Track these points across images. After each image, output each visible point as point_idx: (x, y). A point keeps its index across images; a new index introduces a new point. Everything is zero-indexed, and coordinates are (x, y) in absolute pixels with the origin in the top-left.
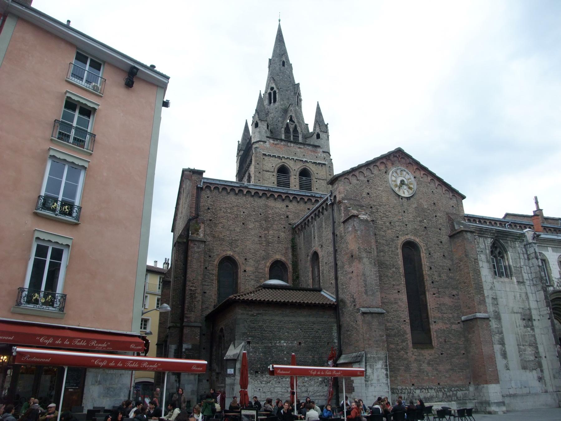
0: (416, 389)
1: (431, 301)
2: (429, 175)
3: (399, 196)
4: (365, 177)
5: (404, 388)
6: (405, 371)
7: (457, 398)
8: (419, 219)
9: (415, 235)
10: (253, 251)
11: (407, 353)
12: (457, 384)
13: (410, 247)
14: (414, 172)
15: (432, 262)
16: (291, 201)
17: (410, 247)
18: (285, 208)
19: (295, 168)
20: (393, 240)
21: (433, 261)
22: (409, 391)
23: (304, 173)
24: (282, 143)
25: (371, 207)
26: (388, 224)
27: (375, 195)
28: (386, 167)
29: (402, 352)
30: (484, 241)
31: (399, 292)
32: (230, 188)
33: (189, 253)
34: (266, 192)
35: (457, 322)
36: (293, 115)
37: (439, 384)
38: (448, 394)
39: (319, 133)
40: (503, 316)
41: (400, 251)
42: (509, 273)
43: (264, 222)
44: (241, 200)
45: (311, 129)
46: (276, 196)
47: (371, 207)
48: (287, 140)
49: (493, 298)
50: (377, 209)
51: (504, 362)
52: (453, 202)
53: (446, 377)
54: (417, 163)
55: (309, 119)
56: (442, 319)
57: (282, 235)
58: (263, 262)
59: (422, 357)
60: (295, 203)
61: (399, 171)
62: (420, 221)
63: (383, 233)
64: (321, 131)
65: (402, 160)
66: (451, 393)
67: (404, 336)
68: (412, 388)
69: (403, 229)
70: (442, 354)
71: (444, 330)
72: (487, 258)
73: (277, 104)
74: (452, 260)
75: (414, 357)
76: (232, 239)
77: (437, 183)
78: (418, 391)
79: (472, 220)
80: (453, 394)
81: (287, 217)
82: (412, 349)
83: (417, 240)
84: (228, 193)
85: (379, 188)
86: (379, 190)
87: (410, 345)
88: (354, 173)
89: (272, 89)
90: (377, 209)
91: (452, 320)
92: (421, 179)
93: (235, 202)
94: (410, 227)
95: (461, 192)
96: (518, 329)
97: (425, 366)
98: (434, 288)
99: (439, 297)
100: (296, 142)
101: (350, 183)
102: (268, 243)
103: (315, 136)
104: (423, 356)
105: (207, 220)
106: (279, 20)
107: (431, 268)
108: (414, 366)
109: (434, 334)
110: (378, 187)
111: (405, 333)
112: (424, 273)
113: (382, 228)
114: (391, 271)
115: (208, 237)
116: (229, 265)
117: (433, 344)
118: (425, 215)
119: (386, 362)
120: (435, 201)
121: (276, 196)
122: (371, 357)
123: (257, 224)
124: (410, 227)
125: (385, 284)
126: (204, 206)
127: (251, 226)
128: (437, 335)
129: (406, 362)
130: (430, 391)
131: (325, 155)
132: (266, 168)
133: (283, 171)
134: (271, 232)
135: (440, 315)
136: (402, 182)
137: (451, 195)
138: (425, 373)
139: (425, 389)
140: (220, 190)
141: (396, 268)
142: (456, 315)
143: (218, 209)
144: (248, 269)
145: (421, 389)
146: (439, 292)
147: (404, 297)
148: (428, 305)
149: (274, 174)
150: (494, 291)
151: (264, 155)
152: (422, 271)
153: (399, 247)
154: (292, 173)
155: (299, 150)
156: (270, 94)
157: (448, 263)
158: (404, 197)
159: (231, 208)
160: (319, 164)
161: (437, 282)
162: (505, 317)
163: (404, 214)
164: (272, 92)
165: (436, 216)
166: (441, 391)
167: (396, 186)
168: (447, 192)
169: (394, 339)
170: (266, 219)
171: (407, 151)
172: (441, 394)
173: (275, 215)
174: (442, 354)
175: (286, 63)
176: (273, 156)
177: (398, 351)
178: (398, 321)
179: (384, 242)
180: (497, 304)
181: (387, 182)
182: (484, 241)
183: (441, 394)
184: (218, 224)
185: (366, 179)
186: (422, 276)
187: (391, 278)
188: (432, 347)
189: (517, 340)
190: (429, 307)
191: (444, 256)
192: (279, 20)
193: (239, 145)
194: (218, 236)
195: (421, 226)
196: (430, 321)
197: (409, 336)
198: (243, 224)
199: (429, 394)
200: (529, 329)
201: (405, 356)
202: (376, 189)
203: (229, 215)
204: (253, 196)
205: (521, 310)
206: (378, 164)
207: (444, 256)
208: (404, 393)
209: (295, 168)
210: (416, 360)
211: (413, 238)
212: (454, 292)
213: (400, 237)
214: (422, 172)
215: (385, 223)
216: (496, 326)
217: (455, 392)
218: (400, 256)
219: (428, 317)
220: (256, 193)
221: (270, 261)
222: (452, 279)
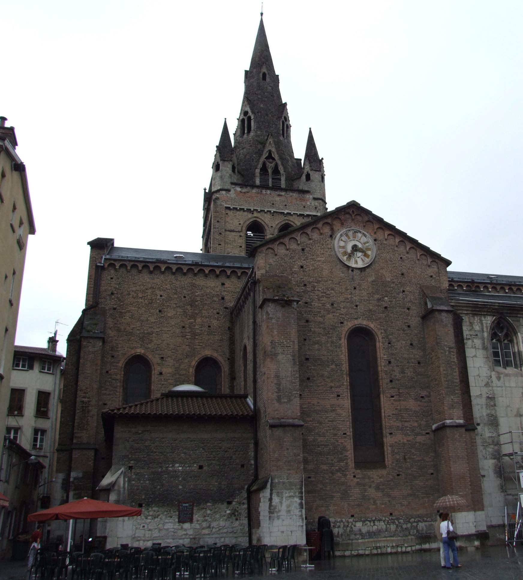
0: (356, 522)
1: (387, 406)
2: (396, 236)
3: (348, 267)
4: (298, 244)
5: (339, 520)
7: (418, 531)
8: (376, 297)
10: (172, 346)
11: (345, 475)
12: (418, 513)
13: (361, 337)
14: (375, 233)
15: (392, 354)
16: (228, 277)
17: (361, 337)
18: (220, 287)
20: (334, 328)
22: (346, 524)
24: (254, 191)
25: (305, 285)
26: (328, 306)
27: (311, 268)
28: (332, 229)
29: (339, 474)
31: (338, 396)
32: (142, 264)
33: (82, 354)
34: (193, 267)
35: (424, 432)
36: (273, 150)
37: (391, 514)
38: (404, 526)
39: (310, 172)
41: (344, 342)
42: (518, 363)
43: (189, 307)
44: (158, 279)
46: (207, 272)
47: (305, 285)
48: (264, 186)
49: (488, 397)
50: (314, 287)
52: (434, 268)
53: (402, 505)
54: (379, 220)
55: (299, 151)
56: (402, 429)
57: (215, 323)
58: (186, 361)
60: (234, 279)
61: (350, 234)
62: (379, 300)
63: (321, 319)
64: (312, 170)
65: (358, 217)
66: (409, 525)
67: (342, 454)
68: (351, 520)
69: (351, 311)
70: (398, 475)
71: (404, 444)
72: (484, 344)
73: (252, 134)
74: (424, 350)
75: (355, 480)
76: (144, 333)
77: (409, 246)
78: (359, 525)
79: (498, 287)
80: (412, 526)
81: (223, 298)
82: (354, 470)
83: (372, 325)
84: (140, 272)
85: (319, 259)
86: (319, 261)
87: (351, 464)
88: (281, 240)
90: (314, 287)
91: (417, 430)
92: (385, 242)
93: (149, 282)
94: (362, 308)
95: (444, 255)
97: (372, 492)
98: (393, 388)
99: (400, 400)
101: (276, 255)
102: (194, 335)
104: (369, 478)
105: (109, 310)
107: (390, 362)
108: (355, 492)
109: (388, 450)
110: (318, 256)
111: (345, 449)
112: (379, 369)
113: (319, 312)
114: (328, 369)
115: (110, 332)
116: (139, 365)
117: (386, 463)
118: (386, 291)
119: (301, 488)
120: (404, 271)
121: (207, 272)
122: (279, 482)
123: (179, 310)
124: (362, 308)
125: (318, 386)
126: (105, 291)
127: (171, 313)
128: (393, 451)
129: (343, 488)
130: (376, 523)
131: (316, 203)
132: (229, 227)
134: (199, 320)
135: (399, 424)
136: (355, 248)
137: (430, 260)
138: (372, 501)
139: (370, 521)
140: (129, 268)
141: (336, 365)
142: (423, 423)
143: (126, 293)
144: (164, 370)
145: (364, 522)
146: (400, 394)
147: (347, 403)
148: (383, 411)
149: (241, 234)
150: (490, 388)
152: (377, 366)
153: (343, 336)
155: (278, 199)
157: (417, 354)
158: (356, 269)
159: (143, 292)
161: (398, 380)
163: (354, 292)
165: (404, 291)
167: (345, 253)
168: (424, 257)
169: (327, 458)
170: (192, 304)
171: (364, 204)
172: (393, 527)
173: (205, 297)
174: (398, 475)
175: (267, 76)
176: (241, 209)
177: (332, 474)
178: (335, 435)
179: (321, 331)
180: (495, 405)
181: (333, 249)
182: (481, 321)
183: (393, 527)
184: (125, 313)
185: (300, 248)
186: (376, 373)
187: (328, 378)
188: (384, 467)
190: (383, 414)
191: (411, 344)
194: (125, 329)
195: (378, 306)
196: (384, 432)
197: (350, 453)
198: (160, 311)
199: (375, 528)
201: (343, 479)
202: (313, 259)
203: (140, 300)
204: (174, 274)
206: (320, 225)
207: (411, 344)
208: (339, 527)
210: (358, 484)
211: (365, 323)
212: (424, 393)
213: (345, 323)
214: (387, 232)
215: (323, 305)
216: (490, 435)
217: (415, 524)
218: (344, 349)
219: (381, 429)
220: (179, 270)
221: (196, 359)
222: (421, 375)
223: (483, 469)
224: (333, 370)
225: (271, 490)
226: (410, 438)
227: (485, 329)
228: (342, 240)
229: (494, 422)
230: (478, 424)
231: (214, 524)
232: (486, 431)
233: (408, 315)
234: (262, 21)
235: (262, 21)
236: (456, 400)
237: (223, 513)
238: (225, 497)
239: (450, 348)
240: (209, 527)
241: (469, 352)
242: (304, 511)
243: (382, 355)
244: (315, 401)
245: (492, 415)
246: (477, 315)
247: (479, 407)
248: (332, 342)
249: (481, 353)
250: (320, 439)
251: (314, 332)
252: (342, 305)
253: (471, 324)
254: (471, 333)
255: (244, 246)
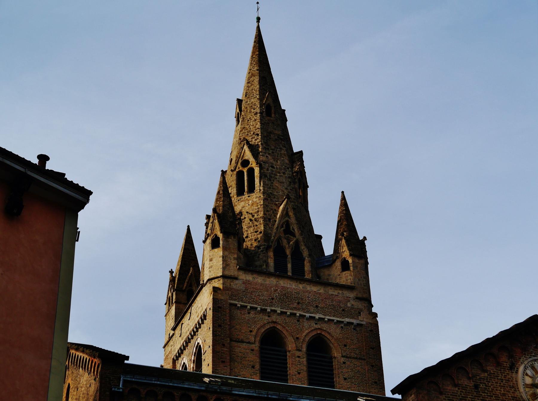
4: (469, 378)
23: (318, 347)
45: (328, 249)
55: (324, 226)
89: (245, 163)
100: (298, 275)
101: (441, 393)
103: (338, 264)
106: (258, 19)
133: (272, 341)
149: (253, 346)
156: (240, 175)
164: (245, 170)
181: (515, 387)
185: (472, 384)
192: (258, 19)
193: (172, 280)
228: (527, 375)
234: (258, 27)
235: (258, 27)
255: (257, 366)
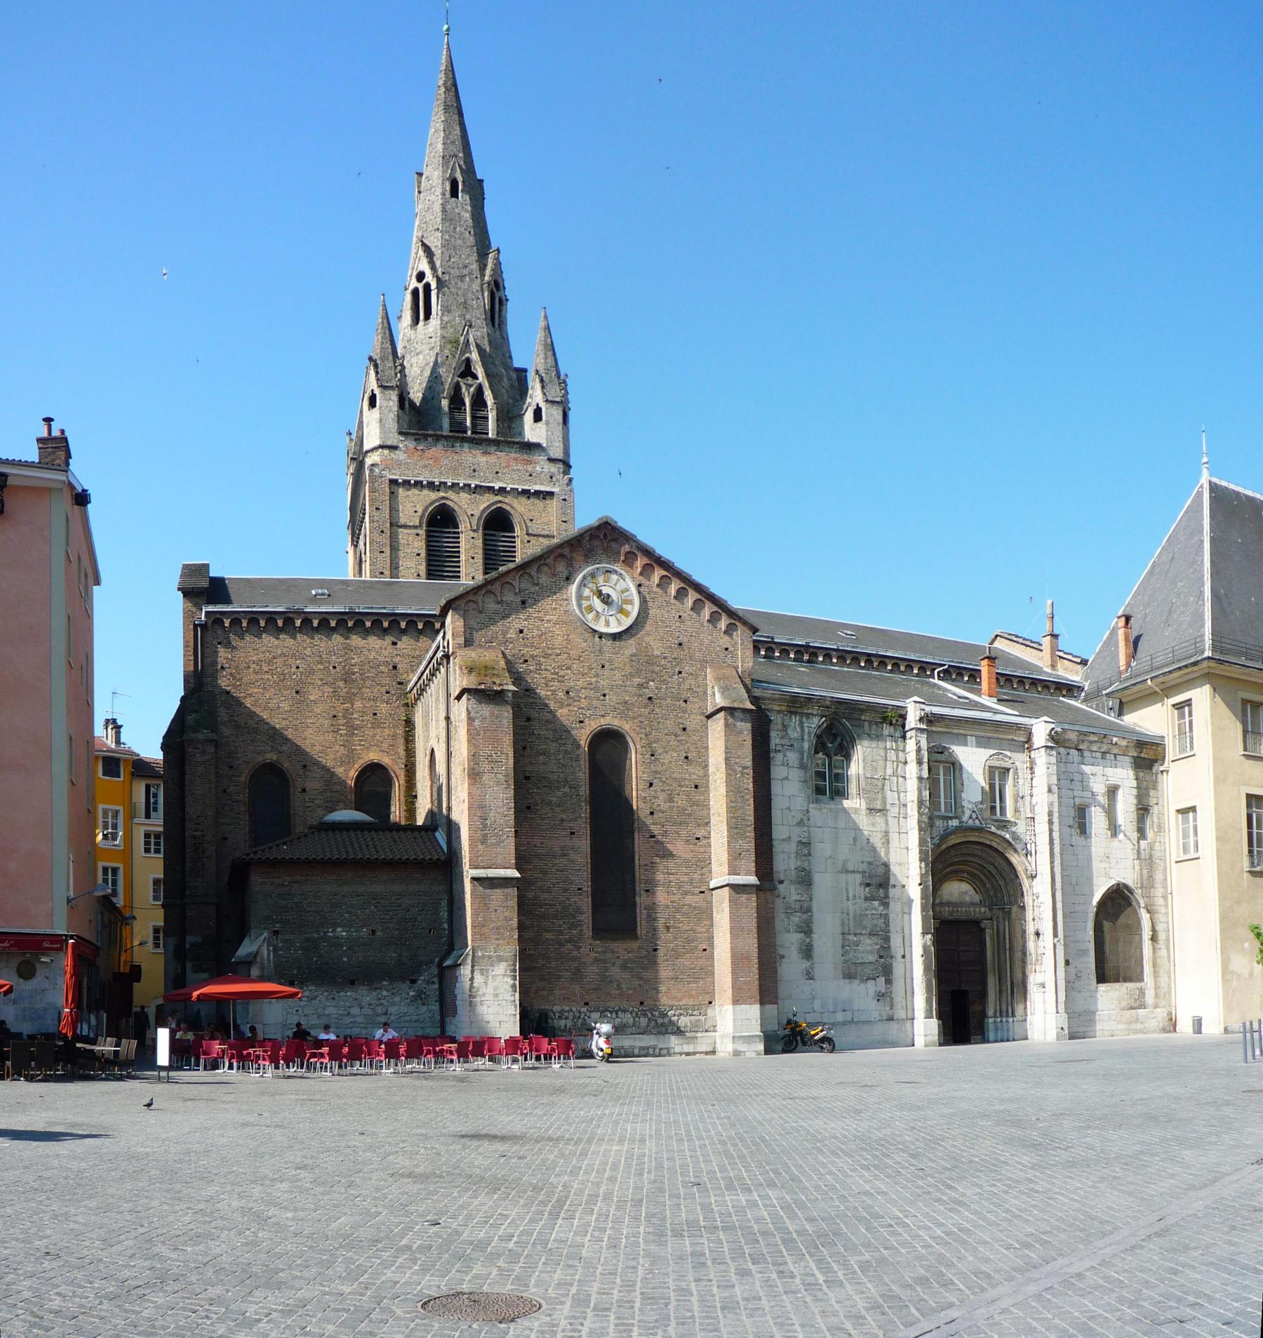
6: (572, 979)
9: (624, 716)
19: (470, 510)
21: (659, 769)
29: (569, 946)
30: (801, 723)
31: (572, 833)
37: (642, 1003)
40: (817, 879)
49: (800, 842)
51: (805, 964)
59: (610, 955)
68: (584, 1009)
72: (802, 759)
82: (591, 941)
87: (588, 932)
91: (687, 887)
96: (850, 903)
97: (615, 972)
104: (613, 952)
107: (651, 785)
108: (592, 971)
111: (579, 911)
125: (543, 819)
129: (574, 965)
130: (620, 1014)
145: (602, 1012)
147: (584, 843)
150: (805, 829)
151: (393, 482)
154: (464, 526)
160: (537, 493)
162: (824, 882)
166: (645, 1015)
172: (644, 1021)
177: (560, 945)
178: (566, 890)
179: (550, 734)
182: (801, 723)
183: (644, 1021)
189: (843, 924)
190: (637, 862)
197: (586, 917)
200: (876, 903)
201: (575, 953)
205: (865, 867)
208: (567, 1018)
209: (470, 510)
210: (596, 960)
216: (798, 897)
219: (634, 882)
223: (781, 946)
224: (565, 794)
225: (473, 966)
226: (675, 898)
227: (806, 737)
229: (805, 880)
230: (781, 882)
231: (393, 1010)
232: (793, 892)
233: (684, 711)
236: (746, 846)
237: (404, 995)
238: (406, 973)
239: (744, 768)
240: (386, 1013)
241: (777, 771)
242: (517, 995)
243: (640, 774)
244: (537, 841)
245: (804, 870)
246: (795, 713)
247: (785, 856)
248: (566, 752)
249: (796, 775)
250: (546, 896)
251: (539, 737)
252: (583, 694)
253: (785, 728)
254: (784, 742)
